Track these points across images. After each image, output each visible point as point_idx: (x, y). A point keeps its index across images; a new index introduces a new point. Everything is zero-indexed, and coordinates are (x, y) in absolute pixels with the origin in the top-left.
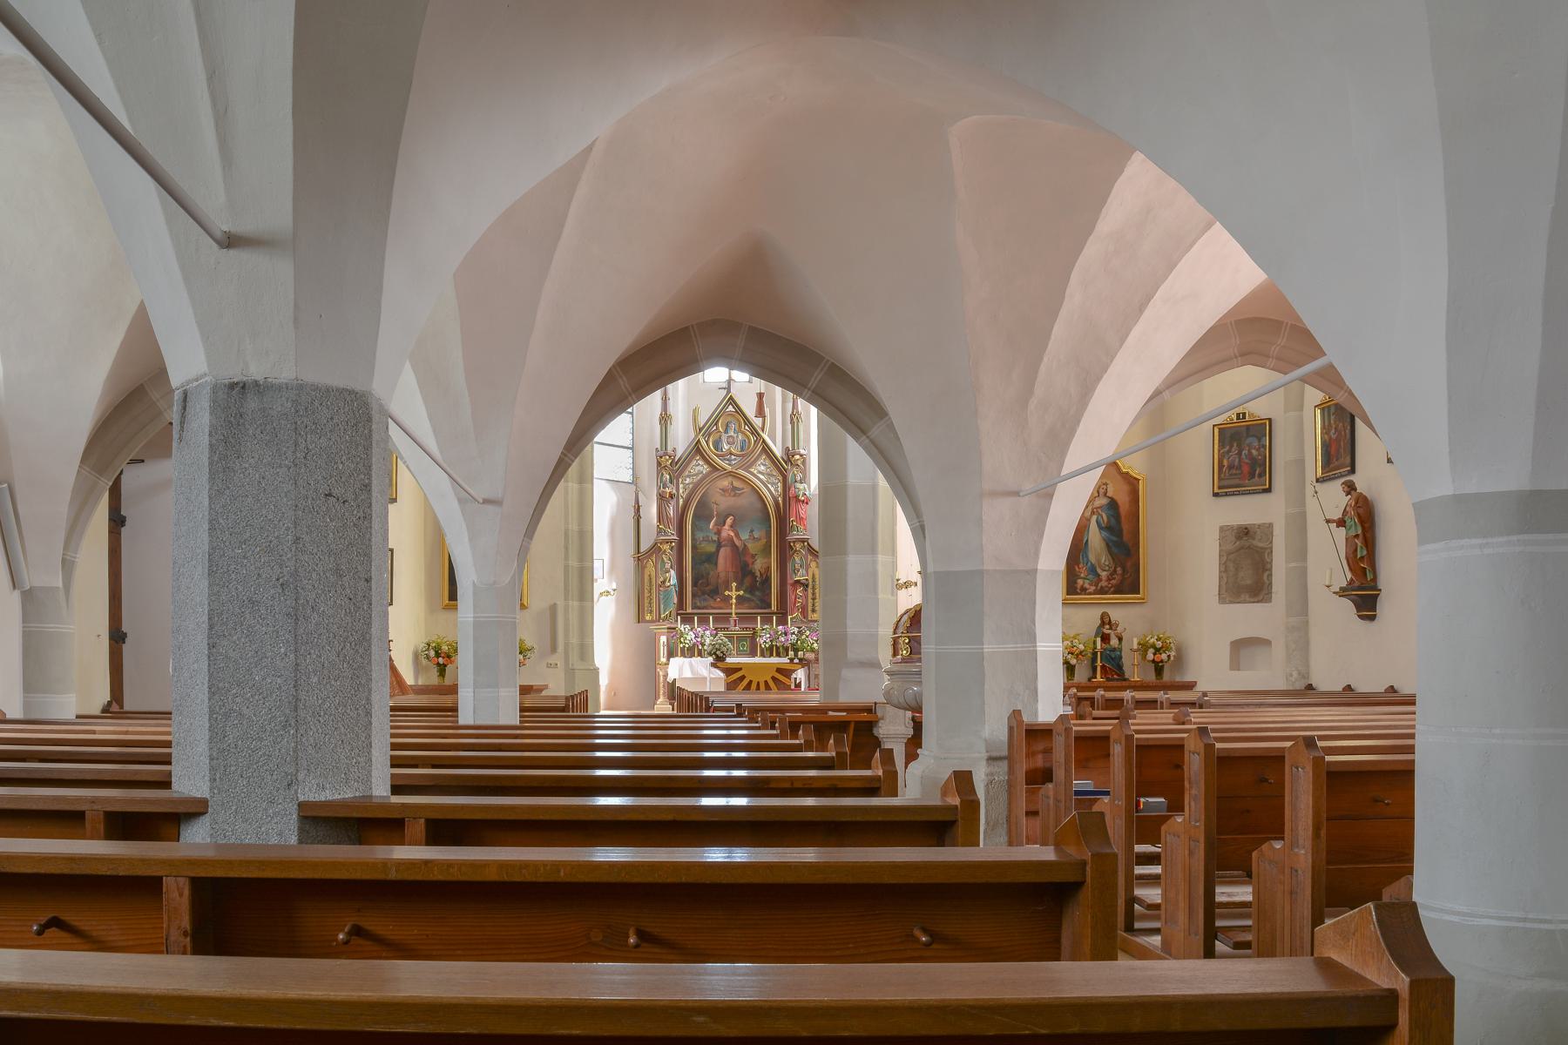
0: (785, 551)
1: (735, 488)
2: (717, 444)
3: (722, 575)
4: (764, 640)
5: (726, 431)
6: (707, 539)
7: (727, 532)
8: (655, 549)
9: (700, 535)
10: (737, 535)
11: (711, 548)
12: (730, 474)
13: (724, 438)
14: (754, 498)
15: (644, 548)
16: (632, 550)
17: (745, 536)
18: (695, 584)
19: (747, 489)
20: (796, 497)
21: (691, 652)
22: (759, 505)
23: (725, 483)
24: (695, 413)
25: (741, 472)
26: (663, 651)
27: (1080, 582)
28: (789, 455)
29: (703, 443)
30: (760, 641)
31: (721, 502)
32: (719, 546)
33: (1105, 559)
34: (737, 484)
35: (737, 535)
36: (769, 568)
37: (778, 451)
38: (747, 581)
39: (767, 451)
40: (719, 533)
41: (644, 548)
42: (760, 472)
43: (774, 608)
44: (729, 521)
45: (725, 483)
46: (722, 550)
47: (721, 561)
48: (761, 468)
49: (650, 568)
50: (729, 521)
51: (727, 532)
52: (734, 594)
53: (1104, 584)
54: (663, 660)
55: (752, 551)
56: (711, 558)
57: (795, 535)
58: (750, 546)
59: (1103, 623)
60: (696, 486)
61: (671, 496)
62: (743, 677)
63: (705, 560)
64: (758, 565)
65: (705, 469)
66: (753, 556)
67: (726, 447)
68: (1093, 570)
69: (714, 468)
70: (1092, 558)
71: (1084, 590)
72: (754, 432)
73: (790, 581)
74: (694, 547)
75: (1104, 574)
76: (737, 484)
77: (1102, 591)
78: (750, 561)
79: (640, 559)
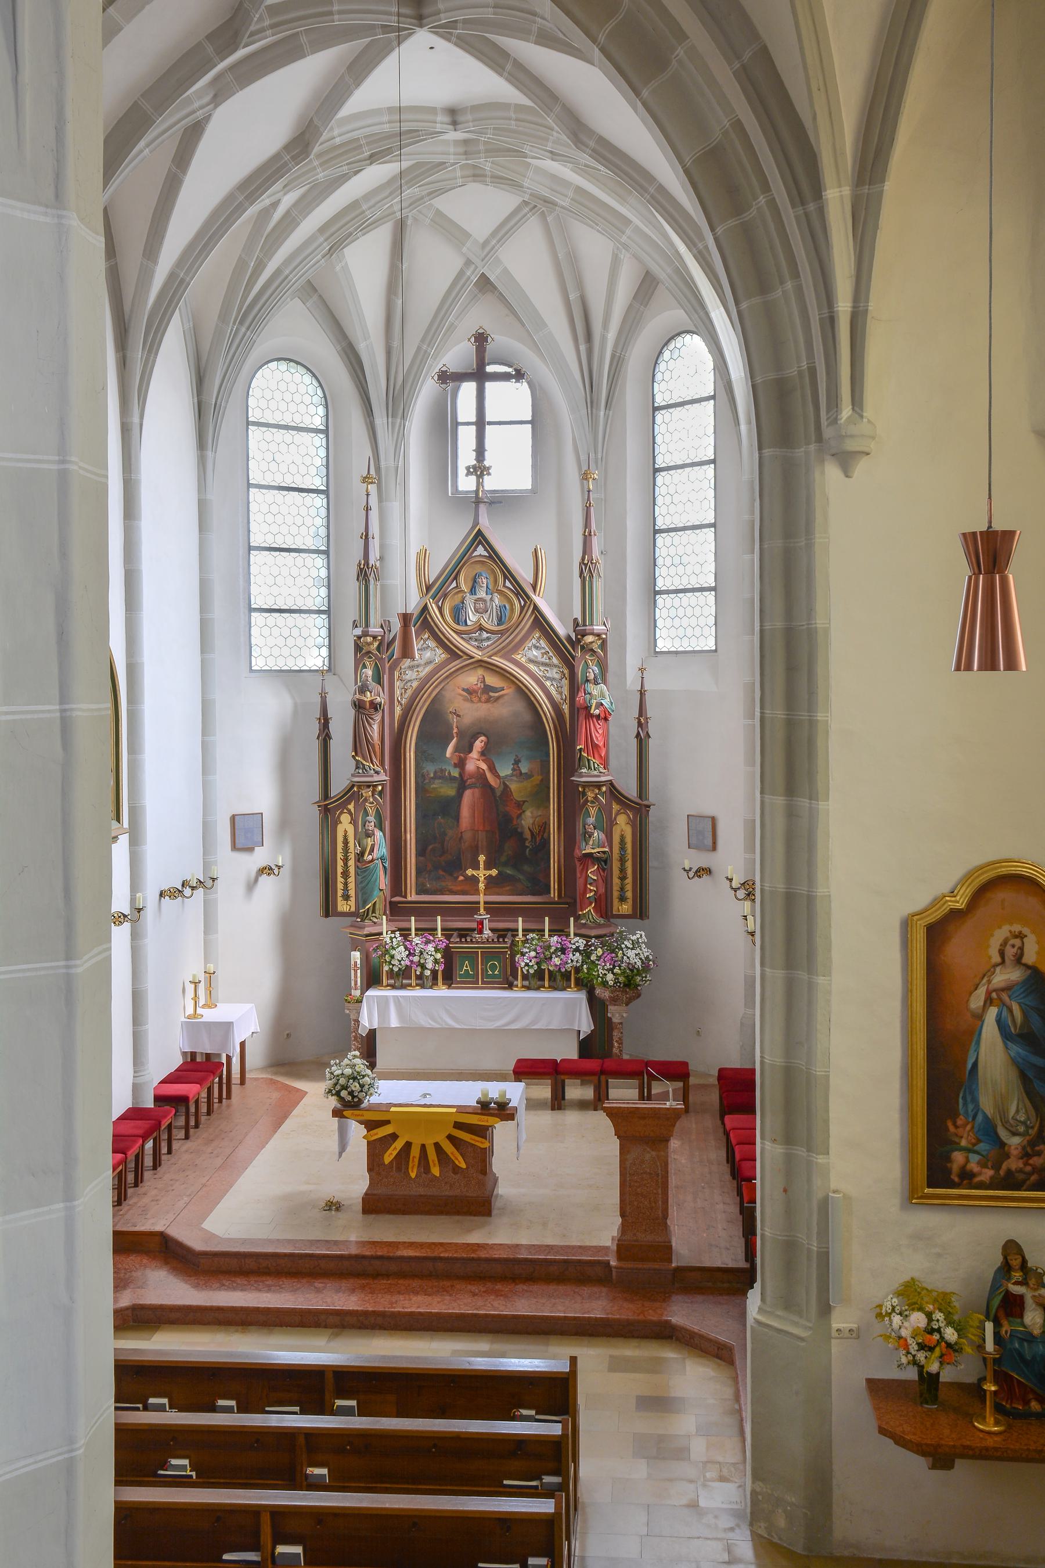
0: (573, 800)
1: (487, 689)
2: (458, 614)
3: (468, 836)
4: (527, 961)
5: (473, 591)
6: (440, 775)
7: (474, 762)
8: (352, 793)
9: (430, 769)
10: (492, 769)
11: (448, 791)
12: (481, 664)
13: (470, 601)
14: (520, 706)
15: (337, 787)
16: (316, 794)
17: (505, 770)
18: (421, 852)
19: (509, 691)
20: (587, 708)
21: (402, 978)
22: (527, 717)
23: (472, 679)
24: (423, 556)
25: (498, 660)
26: (357, 978)
27: (958, 1157)
28: (580, 630)
29: (434, 609)
30: (522, 962)
31: (467, 712)
32: (462, 785)
33: (1016, 1107)
34: (492, 680)
35: (492, 769)
36: (545, 826)
37: (562, 630)
38: (509, 848)
39: (540, 623)
40: (461, 764)
41: (337, 787)
42: (535, 666)
43: (554, 894)
44: (479, 744)
45: (472, 679)
46: (468, 794)
47: (465, 812)
48: (534, 652)
49: (345, 825)
50: (479, 744)
51: (474, 762)
52: (481, 874)
53: (1013, 1164)
54: (357, 993)
55: (517, 796)
56: (449, 808)
57: (585, 776)
58: (513, 786)
59: (1006, 1269)
60: (424, 682)
61: (375, 706)
62: (394, 1137)
63: (437, 810)
64: (528, 819)
65: (439, 655)
66: (519, 805)
67: (472, 618)
68: (989, 1131)
69: (453, 653)
70: (987, 1104)
71: (967, 1178)
72: (520, 591)
73: (577, 853)
74: (420, 789)
75: (1015, 1141)
76: (492, 680)
77: (1009, 1181)
78: (514, 812)
79: (329, 810)
